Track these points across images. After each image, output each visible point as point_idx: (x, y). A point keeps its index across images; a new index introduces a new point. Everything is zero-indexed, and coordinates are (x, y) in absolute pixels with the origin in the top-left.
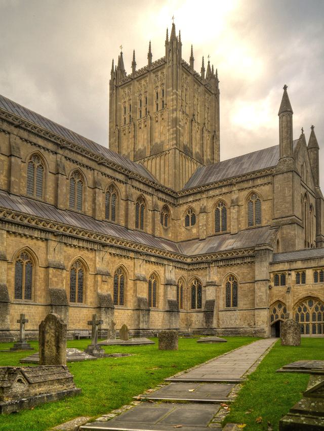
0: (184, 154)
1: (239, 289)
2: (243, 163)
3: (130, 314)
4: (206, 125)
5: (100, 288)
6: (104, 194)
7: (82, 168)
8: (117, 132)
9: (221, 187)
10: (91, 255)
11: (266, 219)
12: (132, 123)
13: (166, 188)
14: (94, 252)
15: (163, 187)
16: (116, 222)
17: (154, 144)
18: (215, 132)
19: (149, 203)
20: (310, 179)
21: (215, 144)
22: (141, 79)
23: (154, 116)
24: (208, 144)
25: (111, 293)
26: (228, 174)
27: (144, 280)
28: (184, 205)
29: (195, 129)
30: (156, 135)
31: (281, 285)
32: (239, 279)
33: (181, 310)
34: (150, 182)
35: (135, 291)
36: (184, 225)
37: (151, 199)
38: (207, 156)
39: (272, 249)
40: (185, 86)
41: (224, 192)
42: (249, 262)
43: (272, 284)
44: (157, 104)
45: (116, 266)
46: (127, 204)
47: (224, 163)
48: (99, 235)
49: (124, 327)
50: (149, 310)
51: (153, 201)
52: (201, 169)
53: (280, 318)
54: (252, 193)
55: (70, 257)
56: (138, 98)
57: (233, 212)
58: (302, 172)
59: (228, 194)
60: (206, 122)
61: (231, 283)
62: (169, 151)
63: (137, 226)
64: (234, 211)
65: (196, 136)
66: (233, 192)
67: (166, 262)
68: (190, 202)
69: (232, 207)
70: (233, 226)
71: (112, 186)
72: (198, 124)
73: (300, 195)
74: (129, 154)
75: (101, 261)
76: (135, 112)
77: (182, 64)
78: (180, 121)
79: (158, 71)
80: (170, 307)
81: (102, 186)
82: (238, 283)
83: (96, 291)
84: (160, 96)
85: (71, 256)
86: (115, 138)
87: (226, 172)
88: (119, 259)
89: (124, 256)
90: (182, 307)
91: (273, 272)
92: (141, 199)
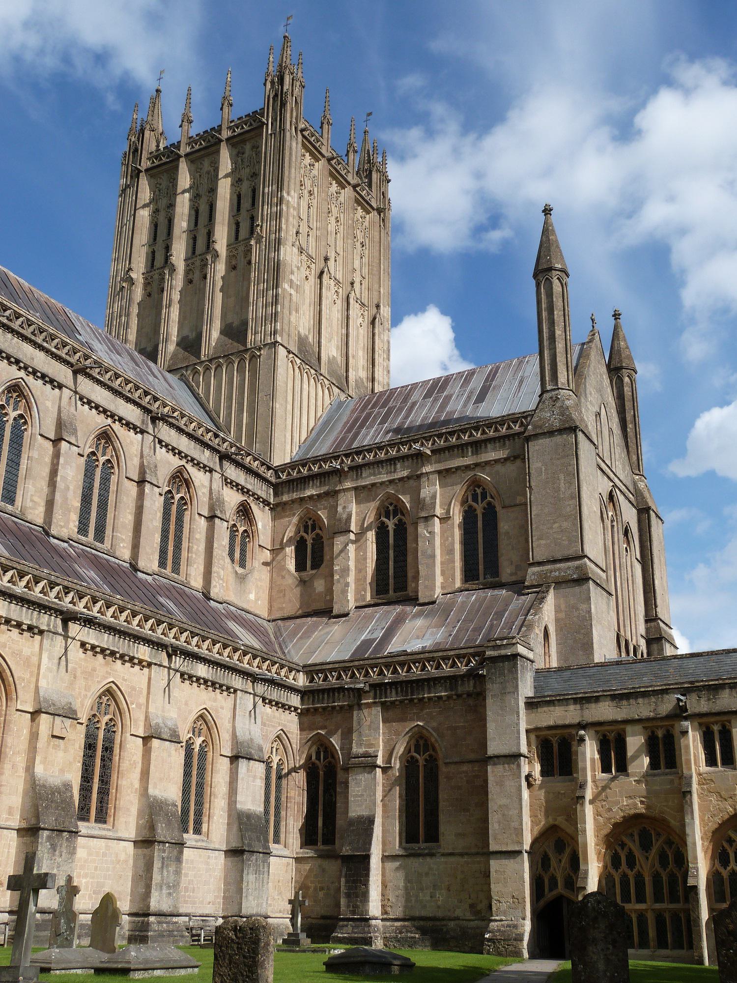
0: (298, 361)
2: (448, 398)
3: (122, 857)
4: (357, 286)
5: (44, 762)
6: (83, 460)
7: (30, 380)
9: (392, 461)
10: (27, 645)
14: (37, 637)
16: (107, 545)
18: (378, 306)
19: (200, 493)
20: (619, 452)
21: (377, 338)
22: (201, 158)
24: (361, 338)
25: (75, 778)
27: (174, 739)
28: (296, 505)
29: (329, 295)
32: (442, 747)
33: (274, 847)
34: (208, 431)
35: (145, 774)
37: (207, 484)
38: (357, 370)
40: (308, 183)
42: (469, 695)
45: (97, 688)
46: (141, 495)
47: (401, 392)
48: (58, 585)
49: (108, 901)
50: (181, 845)
51: (211, 489)
52: (341, 404)
53: (561, 889)
54: (473, 482)
58: (600, 433)
59: (411, 482)
60: (357, 280)
61: (421, 762)
62: (260, 349)
63: (162, 564)
65: (333, 313)
66: (424, 480)
67: (237, 682)
68: (311, 497)
71: (105, 437)
72: (338, 282)
73: (597, 496)
75: (55, 668)
77: (302, 131)
78: (292, 273)
79: (244, 142)
80: (242, 837)
81: (79, 434)
82: (440, 763)
83: (30, 768)
88: (107, 664)
89: (122, 657)
90: (277, 841)
92: (180, 478)
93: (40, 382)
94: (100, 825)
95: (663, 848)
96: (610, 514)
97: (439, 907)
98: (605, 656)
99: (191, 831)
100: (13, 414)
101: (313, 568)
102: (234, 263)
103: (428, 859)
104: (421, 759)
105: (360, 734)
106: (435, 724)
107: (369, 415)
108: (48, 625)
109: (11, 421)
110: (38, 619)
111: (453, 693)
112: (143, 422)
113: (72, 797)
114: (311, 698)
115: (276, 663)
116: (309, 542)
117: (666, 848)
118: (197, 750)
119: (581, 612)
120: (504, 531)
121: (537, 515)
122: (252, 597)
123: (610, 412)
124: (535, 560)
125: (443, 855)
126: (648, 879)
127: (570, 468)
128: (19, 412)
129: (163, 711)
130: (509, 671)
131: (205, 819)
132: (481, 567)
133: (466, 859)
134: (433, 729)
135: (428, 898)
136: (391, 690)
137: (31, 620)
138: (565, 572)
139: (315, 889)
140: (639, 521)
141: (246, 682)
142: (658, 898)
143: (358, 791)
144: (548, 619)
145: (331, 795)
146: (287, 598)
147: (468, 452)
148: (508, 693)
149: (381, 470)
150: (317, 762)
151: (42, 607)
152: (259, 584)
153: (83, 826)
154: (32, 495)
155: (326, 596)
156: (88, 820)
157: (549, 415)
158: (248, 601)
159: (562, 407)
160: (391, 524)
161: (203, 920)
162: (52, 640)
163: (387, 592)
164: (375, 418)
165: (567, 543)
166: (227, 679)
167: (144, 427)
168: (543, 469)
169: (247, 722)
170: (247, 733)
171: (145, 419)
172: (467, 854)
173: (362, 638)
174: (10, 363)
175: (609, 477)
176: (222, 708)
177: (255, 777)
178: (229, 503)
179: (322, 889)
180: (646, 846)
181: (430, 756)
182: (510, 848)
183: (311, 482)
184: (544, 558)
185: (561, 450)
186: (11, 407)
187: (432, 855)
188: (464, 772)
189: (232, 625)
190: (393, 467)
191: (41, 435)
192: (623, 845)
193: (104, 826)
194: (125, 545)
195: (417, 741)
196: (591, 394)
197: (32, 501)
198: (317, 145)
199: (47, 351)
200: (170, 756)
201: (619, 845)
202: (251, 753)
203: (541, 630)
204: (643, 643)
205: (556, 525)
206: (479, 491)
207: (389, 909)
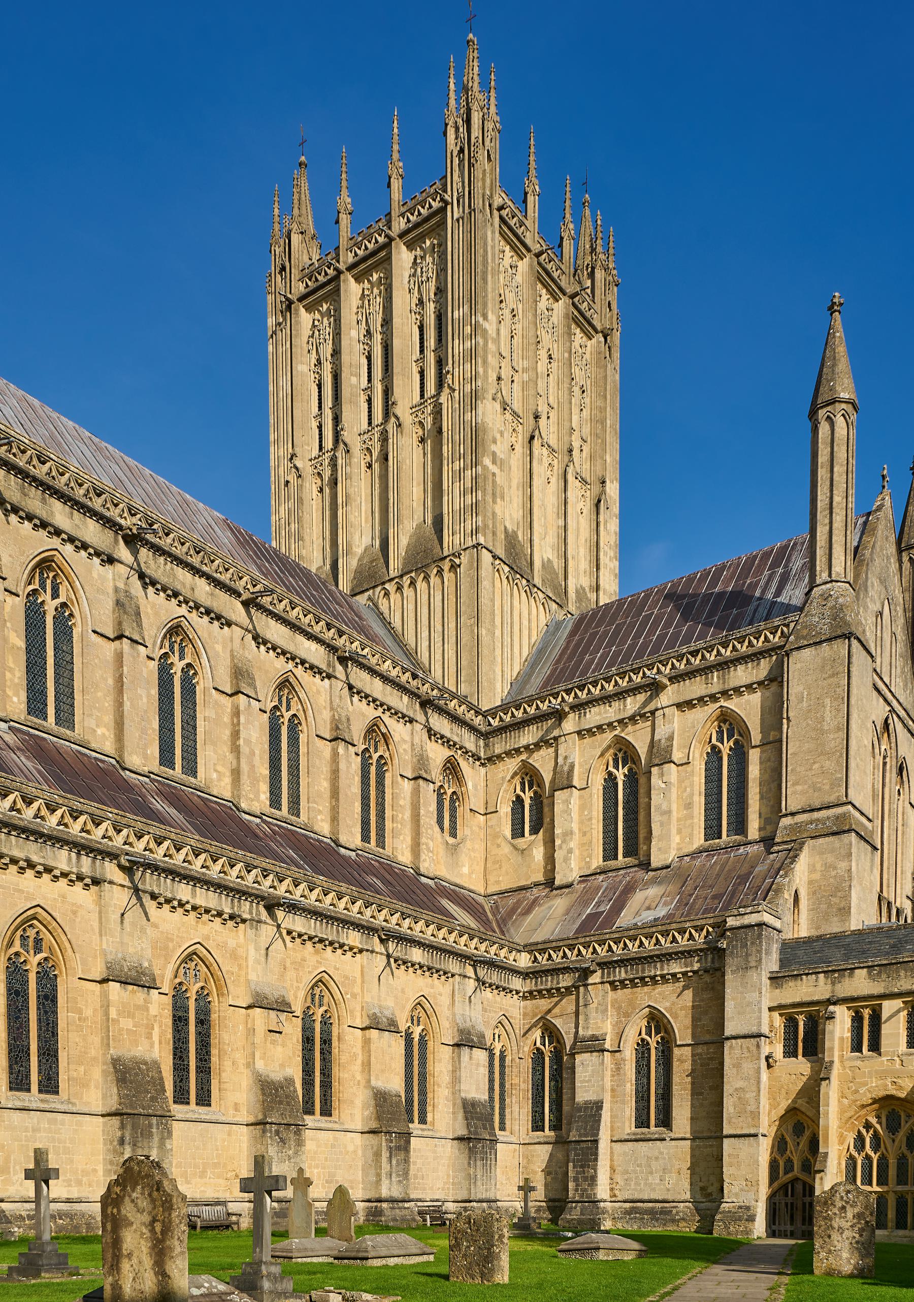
36: (508, 833)
55: (171, 945)
85: (172, 940)
96: (883, 748)
106: (668, 1004)
112: (329, 665)
113: (295, 1091)
115: (494, 943)
124: (789, 811)
129: (379, 1000)
135: (658, 1181)
141: (465, 965)
143: (585, 1076)
146: (504, 869)
158: (462, 875)
163: (616, 858)
165: (827, 787)
169: (468, 1008)
175: (885, 700)
177: (478, 1065)
185: (829, 667)
189: (445, 903)
193: (329, 1119)
199: (208, 577)
203: (790, 895)
205: (816, 766)
207: (617, 1192)
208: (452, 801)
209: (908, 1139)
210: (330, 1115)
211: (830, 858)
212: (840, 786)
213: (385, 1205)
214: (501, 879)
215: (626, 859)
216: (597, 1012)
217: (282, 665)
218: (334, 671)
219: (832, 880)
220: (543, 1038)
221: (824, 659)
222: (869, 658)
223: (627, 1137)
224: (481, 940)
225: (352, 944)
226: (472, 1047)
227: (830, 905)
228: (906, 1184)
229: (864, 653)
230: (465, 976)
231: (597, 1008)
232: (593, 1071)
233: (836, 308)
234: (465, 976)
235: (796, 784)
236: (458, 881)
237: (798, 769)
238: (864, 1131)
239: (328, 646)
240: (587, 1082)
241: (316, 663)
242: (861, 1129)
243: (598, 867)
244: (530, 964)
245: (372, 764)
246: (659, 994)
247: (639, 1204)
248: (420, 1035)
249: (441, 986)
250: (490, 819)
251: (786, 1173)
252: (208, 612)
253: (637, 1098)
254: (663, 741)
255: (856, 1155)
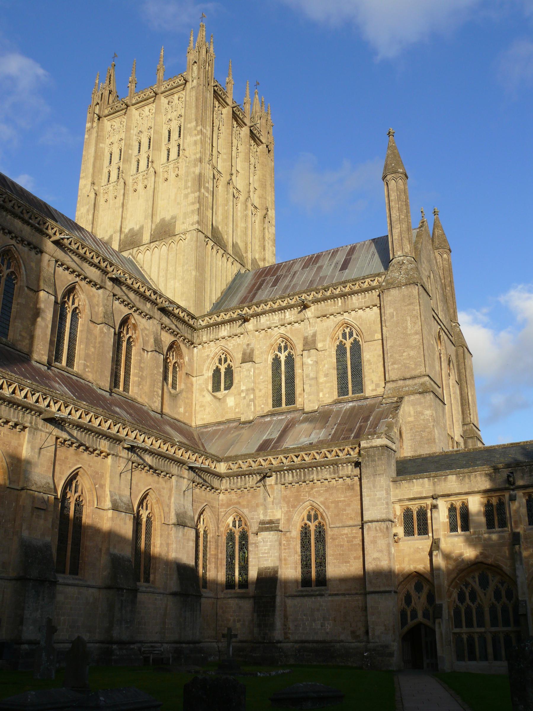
1: (329, 540)
2: (320, 268)
8: (92, 195)
11: (372, 382)
12: (121, 180)
13: (179, 307)
15: (172, 302)
17: (158, 221)
21: (266, 230)
23: (161, 170)
26: (295, 286)
30: (161, 203)
31: (419, 534)
36: (210, 388)
39: (394, 447)
41: (288, 321)
43: (400, 530)
44: (169, 151)
47: (285, 266)
50: (135, 591)
56: (135, 137)
57: (308, 365)
64: (310, 362)
69: (305, 353)
70: (309, 394)
74: (111, 237)
76: (127, 160)
84: (175, 136)
86: (87, 207)
87: (291, 281)
91: (400, 500)
93: (26, 249)
94: (74, 576)
95: (497, 587)
97: (327, 633)
98: (442, 448)
99: (142, 580)
100: (6, 272)
101: (226, 389)
102: (166, 177)
103: (319, 598)
104: (312, 526)
105: (266, 508)
106: (322, 499)
107: (264, 281)
108: (31, 423)
109: (5, 277)
110: (23, 417)
111: (336, 476)
112: (102, 281)
114: (228, 481)
115: (202, 455)
116: (223, 371)
117: (500, 586)
118: (144, 520)
119: (425, 416)
120: (366, 359)
121: (391, 347)
122: (182, 410)
123: (436, 277)
124: (391, 380)
125: (330, 595)
126: (487, 609)
127: (415, 312)
128: (11, 270)
130: (378, 459)
131: (152, 571)
132: (350, 386)
133: (347, 597)
134: (321, 502)
135: (319, 627)
136: (289, 475)
137: (18, 418)
138: (413, 388)
139: (234, 621)
140: (457, 355)
141: (181, 469)
142: (494, 622)
143: (265, 550)
144: (402, 421)
145: (245, 553)
147: (338, 303)
148: (379, 474)
149: (274, 317)
150: (234, 528)
151: (27, 408)
152: (187, 401)
153: (61, 578)
154: (20, 331)
155: (235, 409)
156: (64, 572)
157: (397, 274)
159: (407, 269)
160: (283, 357)
161: (152, 647)
162: (34, 434)
164: (268, 283)
165: (413, 366)
166: (167, 468)
167: (103, 285)
168: (395, 313)
169: (182, 499)
170: (182, 508)
171: (104, 278)
172: (348, 594)
173: (264, 438)
174: (4, 233)
176: (164, 488)
177: (188, 540)
178: (165, 342)
179: (239, 621)
180: (484, 584)
181: (320, 523)
182: (382, 589)
183: (223, 327)
184: (397, 377)
186: (5, 266)
187: (322, 595)
188: (344, 534)
189: (168, 429)
190: (283, 315)
191: (28, 287)
192: (467, 585)
193: (77, 577)
194: (90, 370)
195: (309, 512)
196: (424, 262)
197: (20, 335)
198: (224, 97)
200: (125, 524)
201: (464, 585)
202: (185, 522)
203: (397, 430)
204: (461, 441)
205: (405, 354)
206: (347, 331)
207: (290, 636)
208: (174, 367)
209: (495, 592)
210: (77, 574)
211: (419, 409)
212: (421, 366)
213: (115, 647)
214: (205, 417)
215: (288, 407)
216: (273, 504)
217: (72, 279)
218: (105, 285)
219: (422, 422)
220: (234, 522)
221: (404, 296)
222: (428, 297)
223: (296, 594)
224: (194, 453)
225: (102, 449)
226: (184, 526)
227: (422, 437)
228: (497, 626)
229: (426, 294)
230: (181, 477)
231: (273, 502)
232: (271, 546)
233: (391, 134)
234: (181, 477)
235: (393, 363)
236: (177, 417)
237: (394, 355)
238: (464, 588)
239: (103, 271)
240: (266, 553)
241: (94, 279)
242: (462, 586)
243: (269, 411)
244: (226, 471)
245: (124, 341)
246: (317, 492)
247: (306, 644)
248: (147, 517)
249: (164, 483)
250: (199, 380)
251: (412, 620)
252: (29, 244)
253: (302, 565)
254: (310, 337)
255: (460, 605)
